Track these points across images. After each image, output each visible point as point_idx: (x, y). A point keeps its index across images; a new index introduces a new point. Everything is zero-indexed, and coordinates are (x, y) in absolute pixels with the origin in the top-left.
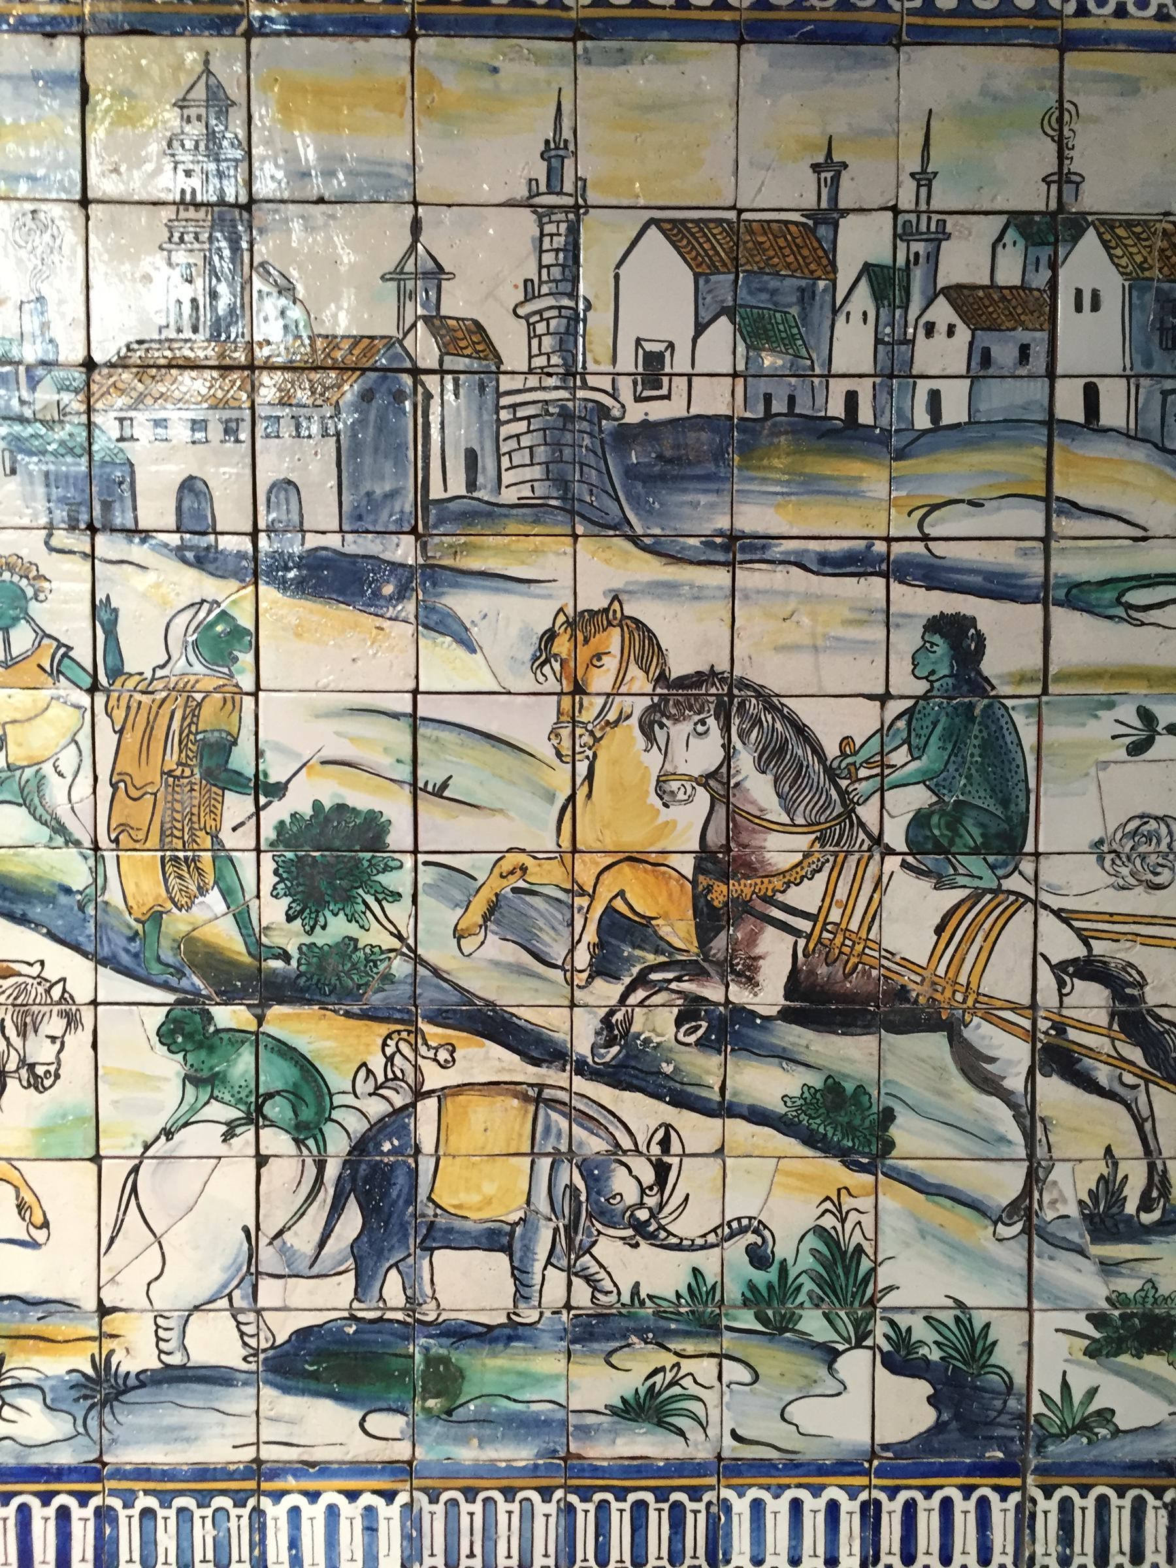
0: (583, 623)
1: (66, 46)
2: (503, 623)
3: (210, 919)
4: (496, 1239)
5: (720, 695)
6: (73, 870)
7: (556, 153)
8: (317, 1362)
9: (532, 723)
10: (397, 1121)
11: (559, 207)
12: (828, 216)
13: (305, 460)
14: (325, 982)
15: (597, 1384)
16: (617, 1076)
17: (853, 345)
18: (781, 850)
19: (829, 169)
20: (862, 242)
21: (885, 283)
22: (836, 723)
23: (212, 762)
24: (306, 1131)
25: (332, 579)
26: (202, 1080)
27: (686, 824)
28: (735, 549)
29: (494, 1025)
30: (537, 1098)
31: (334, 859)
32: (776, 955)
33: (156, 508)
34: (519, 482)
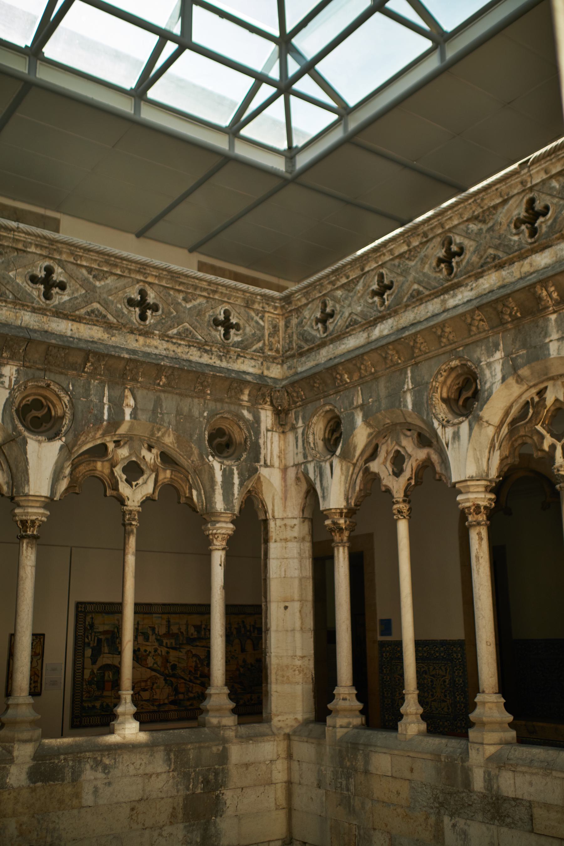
0: (188, 651)
1: (160, 615)
2: (184, 651)
3: (167, 672)
4: (183, 693)
5: (195, 655)
6: (159, 668)
7: (187, 621)
8: (173, 703)
9: (185, 658)
10: (177, 685)
11: (187, 625)
12: (202, 625)
13: (173, 641)
14: (174, 676)
15: (189, 703)
16: (190, 682)
17: (203, 633)
18: (199, 666)
19: (201, 622)
20: (203, 626)
21: (204, 629)
22: (202, 657)
23: (167, 661)
24: (172, 686)
25: (173, 648)
26: (166, 683)
27: (194, 664)
28: (197, 646)
29: (183, 678)
30: (185, 683)
31: (174, 667)
32: (199, 673)
33: (164, 644)
34: (185, 642)
